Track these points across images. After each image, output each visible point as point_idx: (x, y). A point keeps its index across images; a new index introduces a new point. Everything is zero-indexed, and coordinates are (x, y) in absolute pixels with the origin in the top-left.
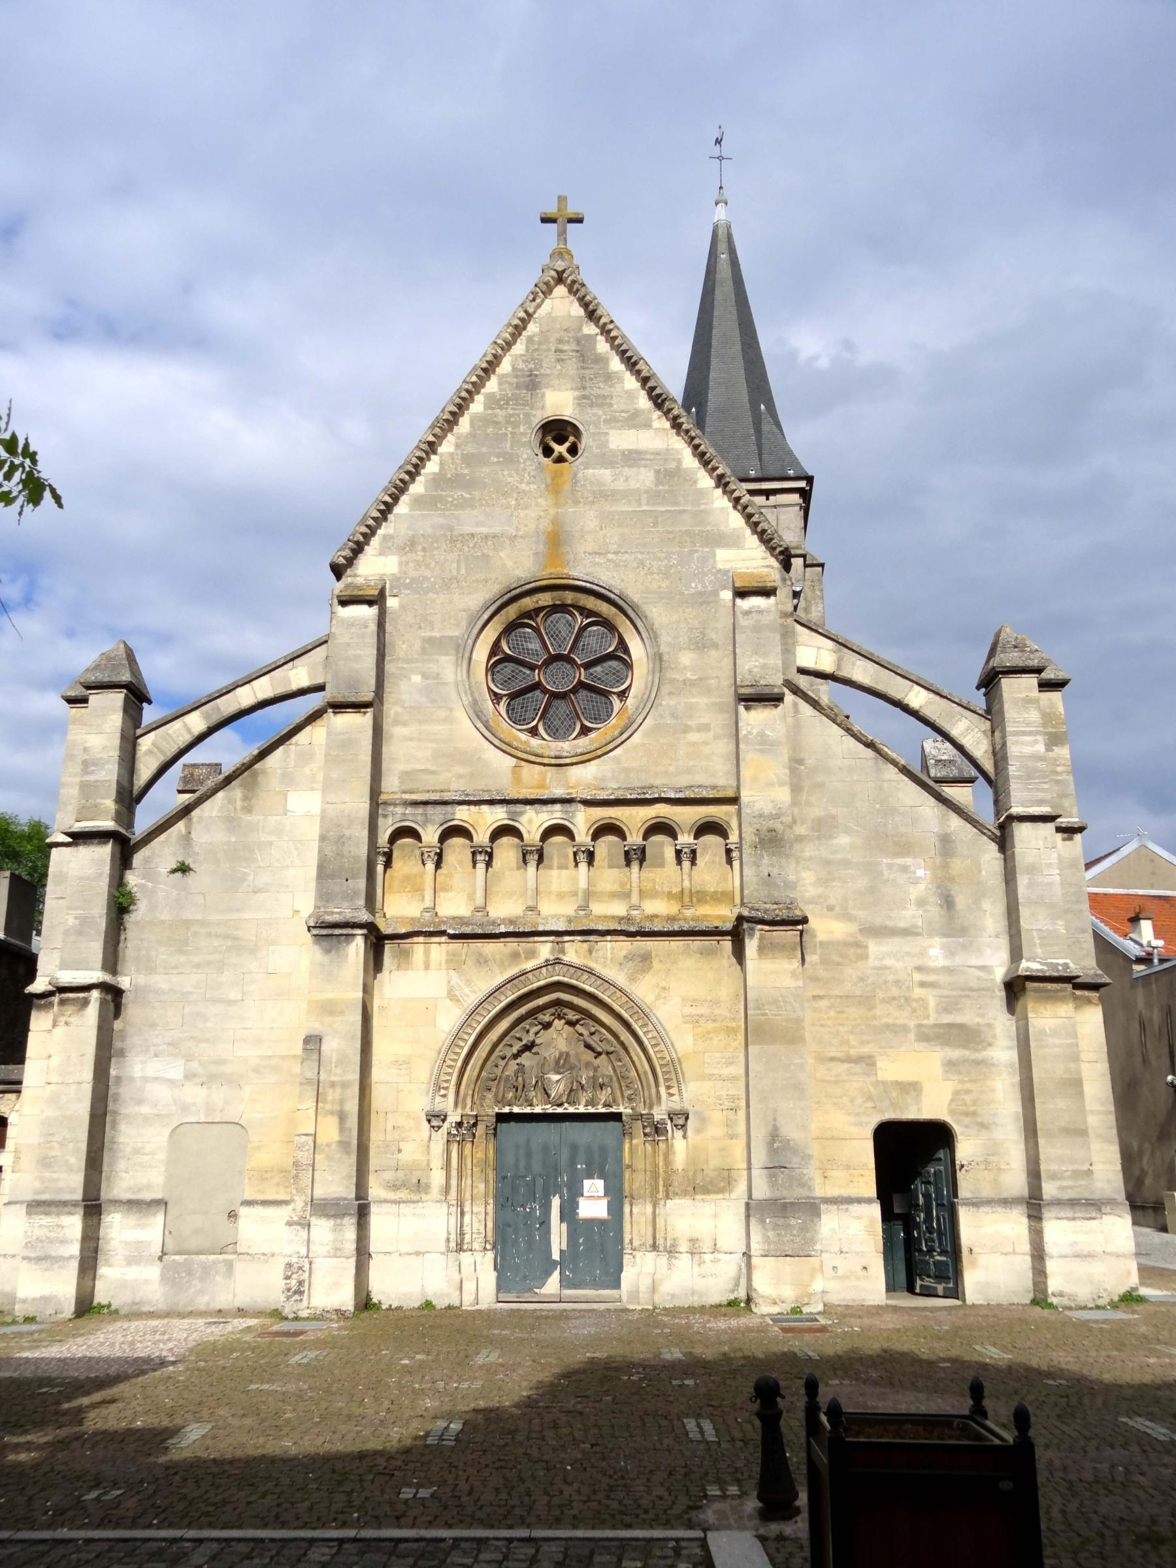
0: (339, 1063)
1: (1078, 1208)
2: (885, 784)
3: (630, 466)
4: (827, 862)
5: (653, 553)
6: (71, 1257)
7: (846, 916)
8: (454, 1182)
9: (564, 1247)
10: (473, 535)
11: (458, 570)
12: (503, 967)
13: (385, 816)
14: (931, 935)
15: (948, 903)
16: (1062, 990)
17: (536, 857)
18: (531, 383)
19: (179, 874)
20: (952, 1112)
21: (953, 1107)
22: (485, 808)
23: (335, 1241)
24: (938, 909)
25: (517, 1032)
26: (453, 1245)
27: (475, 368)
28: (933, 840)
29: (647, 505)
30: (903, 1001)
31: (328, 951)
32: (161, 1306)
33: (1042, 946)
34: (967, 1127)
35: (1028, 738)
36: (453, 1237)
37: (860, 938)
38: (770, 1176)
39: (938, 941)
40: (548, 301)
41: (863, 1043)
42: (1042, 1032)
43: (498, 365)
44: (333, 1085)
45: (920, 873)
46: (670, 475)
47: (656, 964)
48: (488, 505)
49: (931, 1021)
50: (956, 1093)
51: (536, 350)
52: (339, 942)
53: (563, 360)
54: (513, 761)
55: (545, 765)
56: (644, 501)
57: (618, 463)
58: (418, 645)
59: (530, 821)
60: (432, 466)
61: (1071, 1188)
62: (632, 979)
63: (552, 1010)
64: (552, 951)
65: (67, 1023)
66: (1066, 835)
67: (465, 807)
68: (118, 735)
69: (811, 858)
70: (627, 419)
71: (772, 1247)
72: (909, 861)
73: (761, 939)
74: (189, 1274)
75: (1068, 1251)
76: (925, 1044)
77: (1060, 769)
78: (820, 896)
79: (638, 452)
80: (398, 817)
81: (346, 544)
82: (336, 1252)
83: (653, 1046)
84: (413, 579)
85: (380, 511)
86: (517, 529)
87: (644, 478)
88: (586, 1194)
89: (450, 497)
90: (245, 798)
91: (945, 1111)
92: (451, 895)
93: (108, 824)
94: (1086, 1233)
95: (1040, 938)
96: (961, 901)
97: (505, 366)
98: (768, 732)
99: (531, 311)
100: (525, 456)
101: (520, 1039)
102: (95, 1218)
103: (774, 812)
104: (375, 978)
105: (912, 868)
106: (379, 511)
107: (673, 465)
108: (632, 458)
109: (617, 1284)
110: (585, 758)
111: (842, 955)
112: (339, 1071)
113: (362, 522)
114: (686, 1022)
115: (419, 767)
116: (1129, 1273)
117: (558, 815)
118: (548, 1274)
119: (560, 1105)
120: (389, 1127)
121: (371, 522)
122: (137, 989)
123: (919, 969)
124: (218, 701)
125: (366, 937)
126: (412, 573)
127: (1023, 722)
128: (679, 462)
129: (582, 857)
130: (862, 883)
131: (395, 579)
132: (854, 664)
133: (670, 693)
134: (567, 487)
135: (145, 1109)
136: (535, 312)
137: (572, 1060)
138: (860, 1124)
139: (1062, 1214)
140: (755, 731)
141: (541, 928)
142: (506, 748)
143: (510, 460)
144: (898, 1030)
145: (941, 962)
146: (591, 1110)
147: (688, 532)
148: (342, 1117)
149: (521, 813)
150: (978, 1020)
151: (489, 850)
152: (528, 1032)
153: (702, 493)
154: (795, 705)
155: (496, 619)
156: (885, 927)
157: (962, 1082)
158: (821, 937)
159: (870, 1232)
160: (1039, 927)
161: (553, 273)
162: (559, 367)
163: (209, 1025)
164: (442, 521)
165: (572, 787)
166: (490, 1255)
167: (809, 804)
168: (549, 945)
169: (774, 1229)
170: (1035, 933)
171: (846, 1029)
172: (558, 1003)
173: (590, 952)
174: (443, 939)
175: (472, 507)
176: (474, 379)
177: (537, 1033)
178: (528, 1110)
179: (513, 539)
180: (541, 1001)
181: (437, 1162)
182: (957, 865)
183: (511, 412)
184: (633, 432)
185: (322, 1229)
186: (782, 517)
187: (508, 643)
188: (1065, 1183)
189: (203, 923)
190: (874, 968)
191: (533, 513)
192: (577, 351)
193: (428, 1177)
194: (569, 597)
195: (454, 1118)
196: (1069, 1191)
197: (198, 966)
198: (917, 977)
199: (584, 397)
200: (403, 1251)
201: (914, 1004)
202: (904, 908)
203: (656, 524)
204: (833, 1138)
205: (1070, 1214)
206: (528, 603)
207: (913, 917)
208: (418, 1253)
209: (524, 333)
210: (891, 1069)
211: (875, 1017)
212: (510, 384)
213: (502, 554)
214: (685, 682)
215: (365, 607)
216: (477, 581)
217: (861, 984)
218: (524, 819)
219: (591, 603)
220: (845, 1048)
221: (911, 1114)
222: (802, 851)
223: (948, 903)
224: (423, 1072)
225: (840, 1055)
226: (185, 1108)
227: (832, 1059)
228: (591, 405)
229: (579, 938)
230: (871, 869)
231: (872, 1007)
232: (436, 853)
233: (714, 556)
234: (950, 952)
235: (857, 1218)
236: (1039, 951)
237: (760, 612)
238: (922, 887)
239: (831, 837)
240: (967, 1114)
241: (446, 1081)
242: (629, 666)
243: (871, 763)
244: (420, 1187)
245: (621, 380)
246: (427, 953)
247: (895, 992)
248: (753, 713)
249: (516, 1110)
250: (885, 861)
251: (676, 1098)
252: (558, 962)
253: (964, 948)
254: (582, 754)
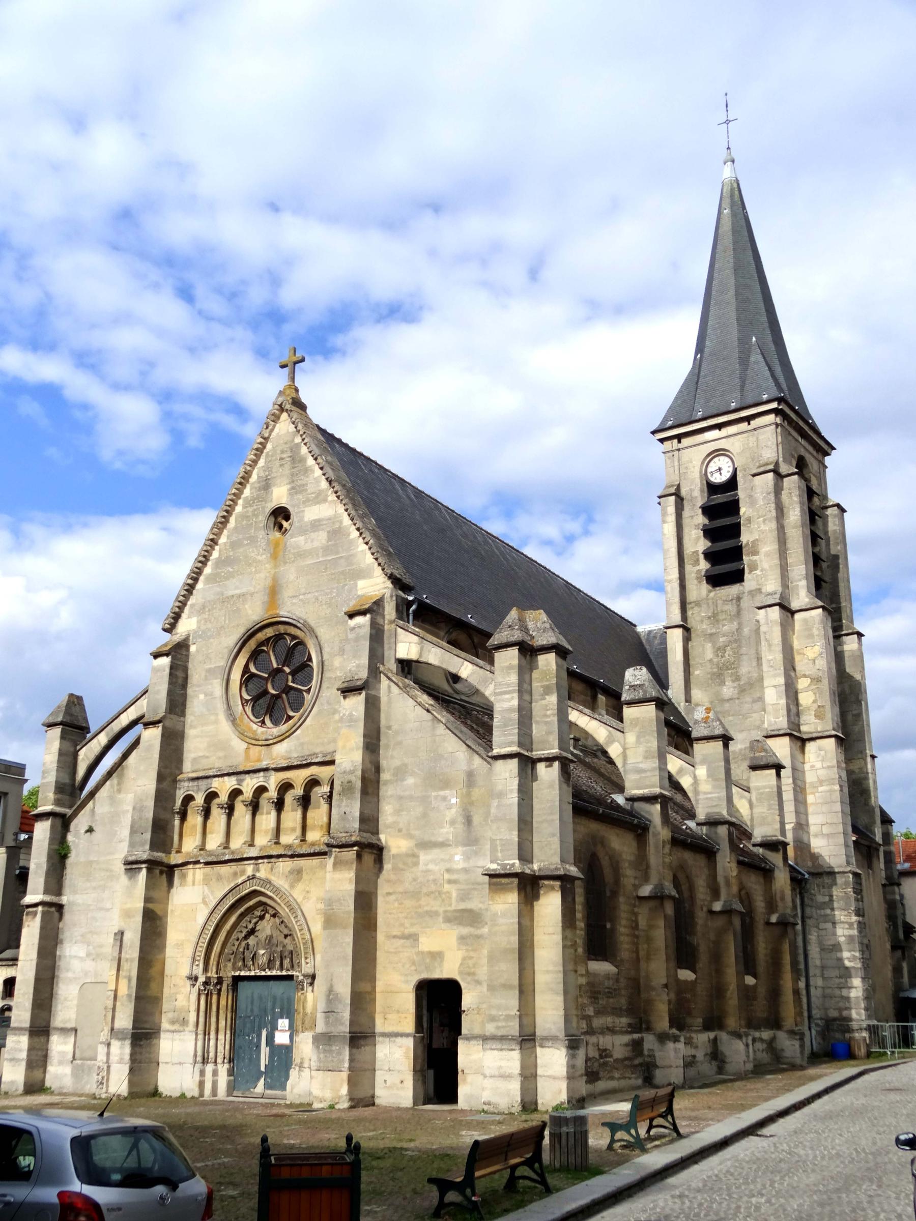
0: (131, 947)
1: (504, 1042)
2: (437, 738)
3: (314, 531)
4: (400, 798)
5: (323, 590)
6: (23, 1059)
7: (409, 836)
8: (202, 1020)
9: (267, 1063)
10: (233, 596)
11: (225, 621)
12: (229, 882)
13: (180, 789)
14: (456, 846)
15: (468, 821)
16: (512, 883)
18: (266, 485)
19: (89, 833)
20: (461, 973)
21: (462, 969)
22: (226, 778)
23: (121, 1054)
24: (462, 826)
25: (243, 923)
26: (199, 1059)
27: (234, 485)
28: (462, 777)
29: (323, 556)
30: (437, 894)
31: (130, 878)
32: (71, 1090)
33: (502, 851)
34: (468, 983)
35: (507, 696)
36: (199, 1053)
37: (416, 850)
38: (327, 1018)
39: (460, 849)
40: (278, 425)
41: (412, 925)
42: (495, 914)
43: (250, 476)
44: (127, 960)
45: (454, 801)
46: (336, 533)
47: (305, 876)
48: (241, 574)
49: (453, 908)
50: (464, 959)
51: (270, 461)
52: (135, 873)
53: (283, 465)
54: (245, 745)
55: (261, 746)
56: (320, 555)
57: (307, 530)
58: (203, 674)
59: (248, 785)
60: (215, 554)
61: (503, 1027)
62: (292, 886)
63: (261, 908)
64: (253, 870)
65: (28, 926)
66: (548, 763)
67: (216, 779)
68: (57, 754)
69: (391, 796)
70: (317, 497)
71: (322, 1065)
72: (447, 792)
73: (336, 857)
74: (83, 1071)
75: (497, 1073)
76: (448, 924)
77: (549, 713)
78: (394, 822)
79: (319, 520)
80: (186, 789)
81: (168, 615)
82: (121, 1061)
83: (301, 930)
84: (203, 632)
85: (186, 590)
86: (255, 587)
87: (321, 538)
88: (279, 1028)
89: (222, 572)
90: (119, 784)
91: (457, 972)
92: (214, 835)
94: (508, 1060)
95: (502, 845)
96: (477, 819)
97: (254, 478)
98: (354, 713)
99: (266, 435)
100: (261, 537)
101: (247, 928)
102: (43, 1039)
103: (352, 769)
104: (169, 892)
105: (449, 797)
106: (186, 590)
107: (337, 526)
108: (316, 525)
109: (283, 1087)
110: (282, 738)
111: (405, 864)
112: (130, 952)
113: (177, 600)
114: (318, 914)
115: (201, 754)
116: (560, 1091)
117: (261, 779)
118: (258, 1079)
119: (264, 970)
120: (172, 986)
121: (181, 598)
122: (69, 902)
123: (448, 871)
124: (112, 724)
125: (149, 870)
126: (203, 627)
127: (506, 684)
128: (341, 522)
129: (272, 806)
130: (419, 810)
131: (195, 632)
132: (429, 651)
133: (328, 688)
134: (281, 553)
135: (70, 975)
136: (270, 435)
137: (274, 941)
138: (407, 982)
139: (494, 1047)
140: (347, 713)
141: (245, 856)
142: (242, 735)
143: (253, 540)
144: (433, 914)
145: (461, 865)
146: (279, 973)
147: (343, 573)
148: (130, 980)
149: (243, 780)
150: (481, 905)
152: (250, 922)
153: (351, 542)
154: (389, 687)
155: (243, 650)
156: (430, 842)
157: (467, 951)
158: (394, 851)
159: (407, 1057)
160: (501, 837)
161: (277, 407)
162: (281, 470)
163: (98, 924)
164: (218, 589)
165: (274, 759)
166: (226, 1066)
167: (392, 757)
168: (252, 866)
169: (324, 1053)
170: (498, 842)
171: (403, 915)
173: (272, 869)
174: (201, 865)
175: (233, 577)
176: (234, 491)
177: (256, 923)
178: (248, 974)
179: (252, 594)
180: (251, 903)
181: (193, 1007)
182: (476, 793)
183: (255, 507)
184: (318, 506)
185: (116, 1045)
186: (761, 438)
187: (255, 664)
188: (500, 1024)
189: (97, 862)
190: (422, 871)
191: (262, 575)
192: (290, 457)
193: (188, 1016)
194: (282, 629)
195: (202, 979)
196: (502, 1030)
197: (94, 888)
198: (446, 876)
199: (293, 488)
200: (174, 1062)
201: (444, 896)
202: (442, 828)
203: (326, 569)
204: (391, 992)
205: (499, 1046)
206: (261, 636)
207: (447, 833)
208: (180, 1064)
209: (265, 451)
210: (427, 943)
211: (420, 906)
212: (256, 488)
213: (246, 606)
214: (335, 678)
215: (165, 658)
216: (234, 627)
217: (414, 883)
218: (245, 784)
219: (292, 631)
220: (402, 929)
221: (436, 975)
222: (387, 791)
223: (468, 821)
224: (189, 951)
225: (399, 934)
226: (86, 974)
227: (395, 937)
228: (296, 493)
229: (266, 861)
230: (424, 800)
231: (419, 899)
233: (356, 586)
234: (467, 858)
235: (400, 1047)
236: (499, 855)
237: (360, 627)
238: (454, 810)
239: (403, 780)
240: (469, 974)
241: (199, 956)
242: (313, 669)
243: (430, 724)
244: (184, 1022)
245: (313, 471)
246: (194, 875)
247: (433, 887)
248: (347, 700)
249: (243, 973)
250: (433, 794)
251: (309, 965)
252: (254, 877)
253: (476, 853)
254: (279, 736)
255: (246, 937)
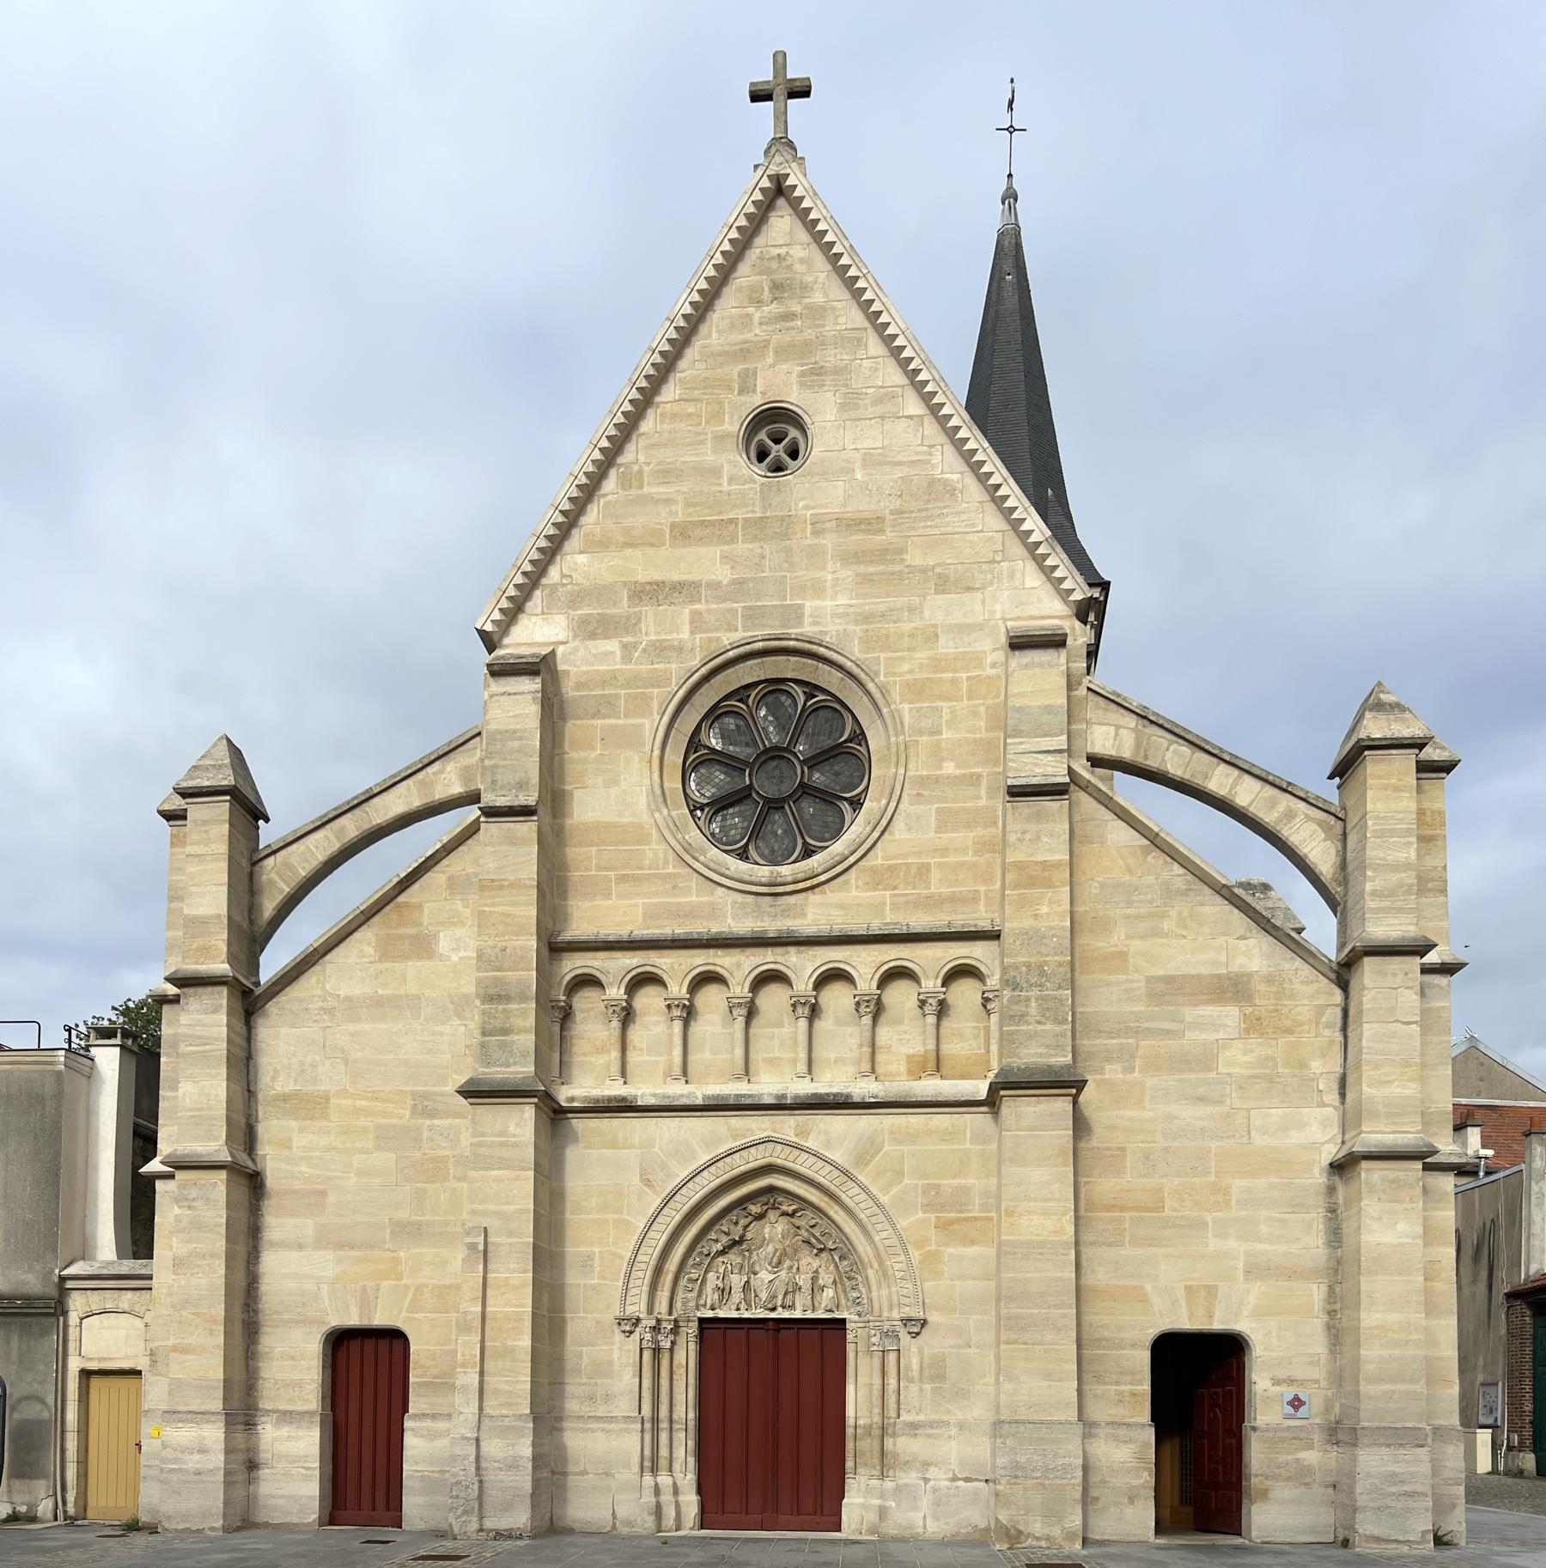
17: (744, 1012)
63: (764, 1199)
93: (222, 967)
101: (728, 1234)
146: (809, 1315)
151: (687, 1003)
152: (736, 1223)
172: (771, 1189)
177: (746, 1227)
232: (623, 1009)
255: (723, 1252)
